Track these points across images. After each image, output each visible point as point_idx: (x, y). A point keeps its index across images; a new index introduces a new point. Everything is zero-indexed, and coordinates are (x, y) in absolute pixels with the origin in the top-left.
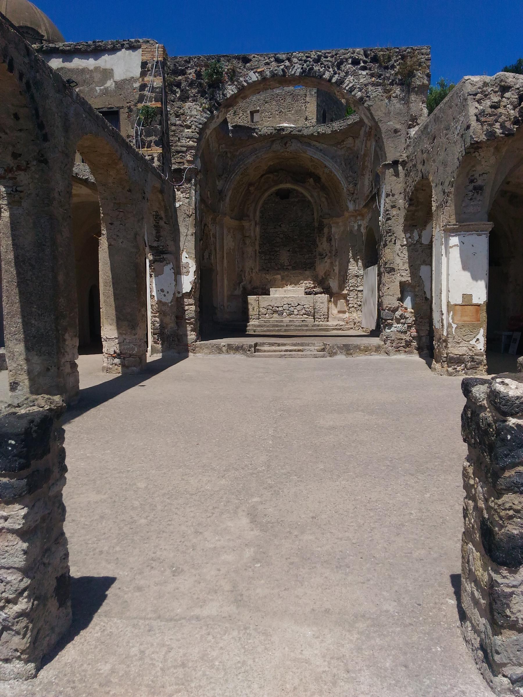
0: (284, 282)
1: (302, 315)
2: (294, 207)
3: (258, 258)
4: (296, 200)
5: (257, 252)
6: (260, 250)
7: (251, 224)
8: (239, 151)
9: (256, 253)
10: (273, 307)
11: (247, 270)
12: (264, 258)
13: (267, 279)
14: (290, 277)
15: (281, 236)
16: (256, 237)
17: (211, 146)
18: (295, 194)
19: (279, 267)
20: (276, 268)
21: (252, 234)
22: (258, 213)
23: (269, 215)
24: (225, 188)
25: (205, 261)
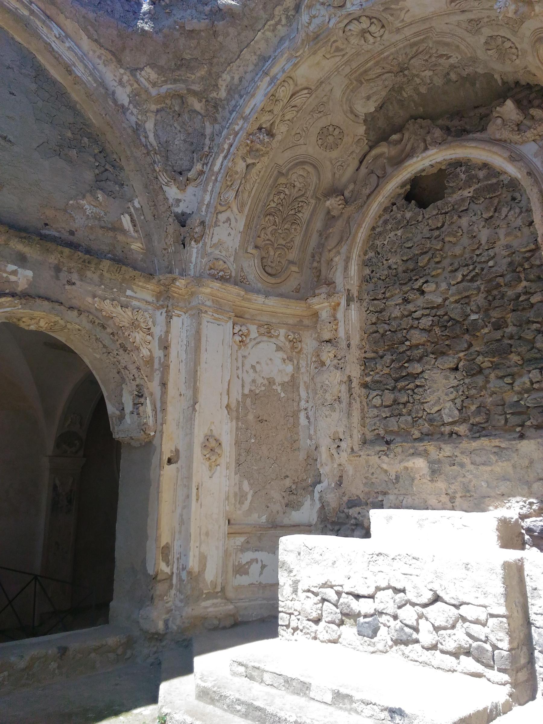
0: (441, 485)
1: (456, 654)
2: (460, 217)
3: (356, 406)
4: (467, 193)
5: (355, 384)
6: (368, 379)
7: (339, 304)
8: (223, 85)
9: (350, 389)
10: (339, 594)
11: (325, 443)
12: (377, 401)
13: (386, 471)
14: (462, 465)
15: (426, 322)
16: (348, 338)
17: (79, 70)
18: (463, 176)
19: (426, 427)
20: (417, 434)
21: (341, 333)
22: (354, 269)
23: (390, 267)
24: (201, 203)
25: (128, 419)
